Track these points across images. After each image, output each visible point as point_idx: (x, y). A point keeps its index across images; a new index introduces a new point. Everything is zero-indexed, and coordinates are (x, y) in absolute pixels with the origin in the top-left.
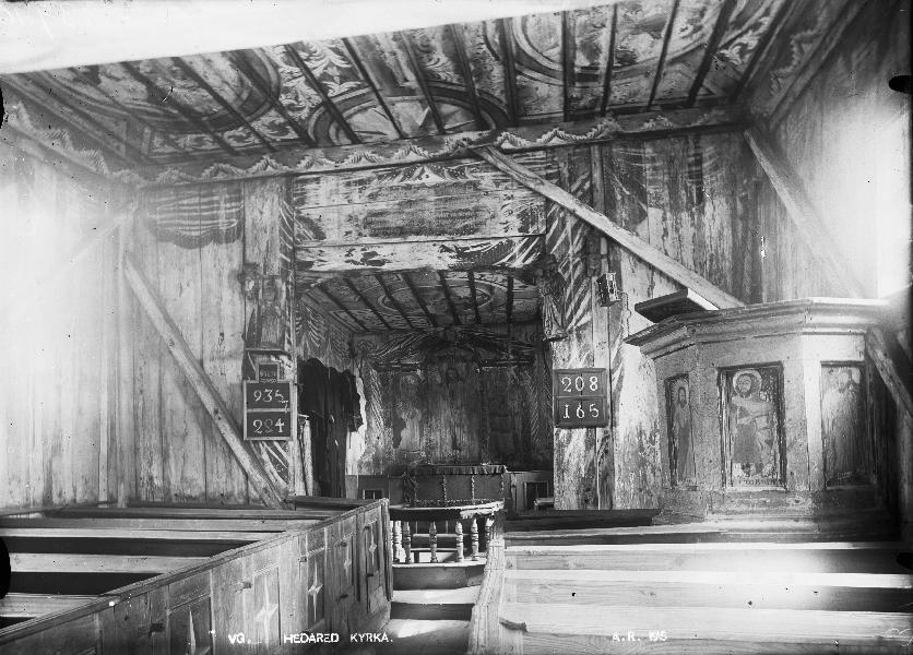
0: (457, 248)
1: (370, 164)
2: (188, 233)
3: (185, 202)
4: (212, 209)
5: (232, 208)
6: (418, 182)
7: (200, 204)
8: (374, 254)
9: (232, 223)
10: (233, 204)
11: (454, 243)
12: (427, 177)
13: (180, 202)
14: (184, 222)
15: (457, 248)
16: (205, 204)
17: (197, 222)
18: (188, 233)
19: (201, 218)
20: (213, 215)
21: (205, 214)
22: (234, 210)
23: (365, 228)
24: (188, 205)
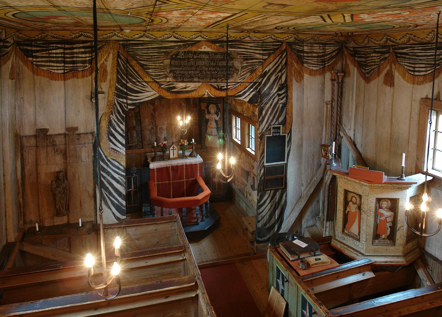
0: (218, 86)
1: (175, 39)
2: (56, 71)
3: (54, 51)
4: (73, 57)
5: (86, 57)
6: (199, 50)
7: (64, 53)
8: (174, 88)
9: (87, 66)
10: (88, 55)
11: (217, 84)
12: (205, 48)
13: (50, 52)
14: (53, 64)
15: (218, 86)
16: (67, 54)
17: (63, 65)
18: (56, 71)
19: (65, 62)
20: (74, 61)
21: (68, 60)
22: (87, 59)
23: (170, 73)
24: (56, 53)
